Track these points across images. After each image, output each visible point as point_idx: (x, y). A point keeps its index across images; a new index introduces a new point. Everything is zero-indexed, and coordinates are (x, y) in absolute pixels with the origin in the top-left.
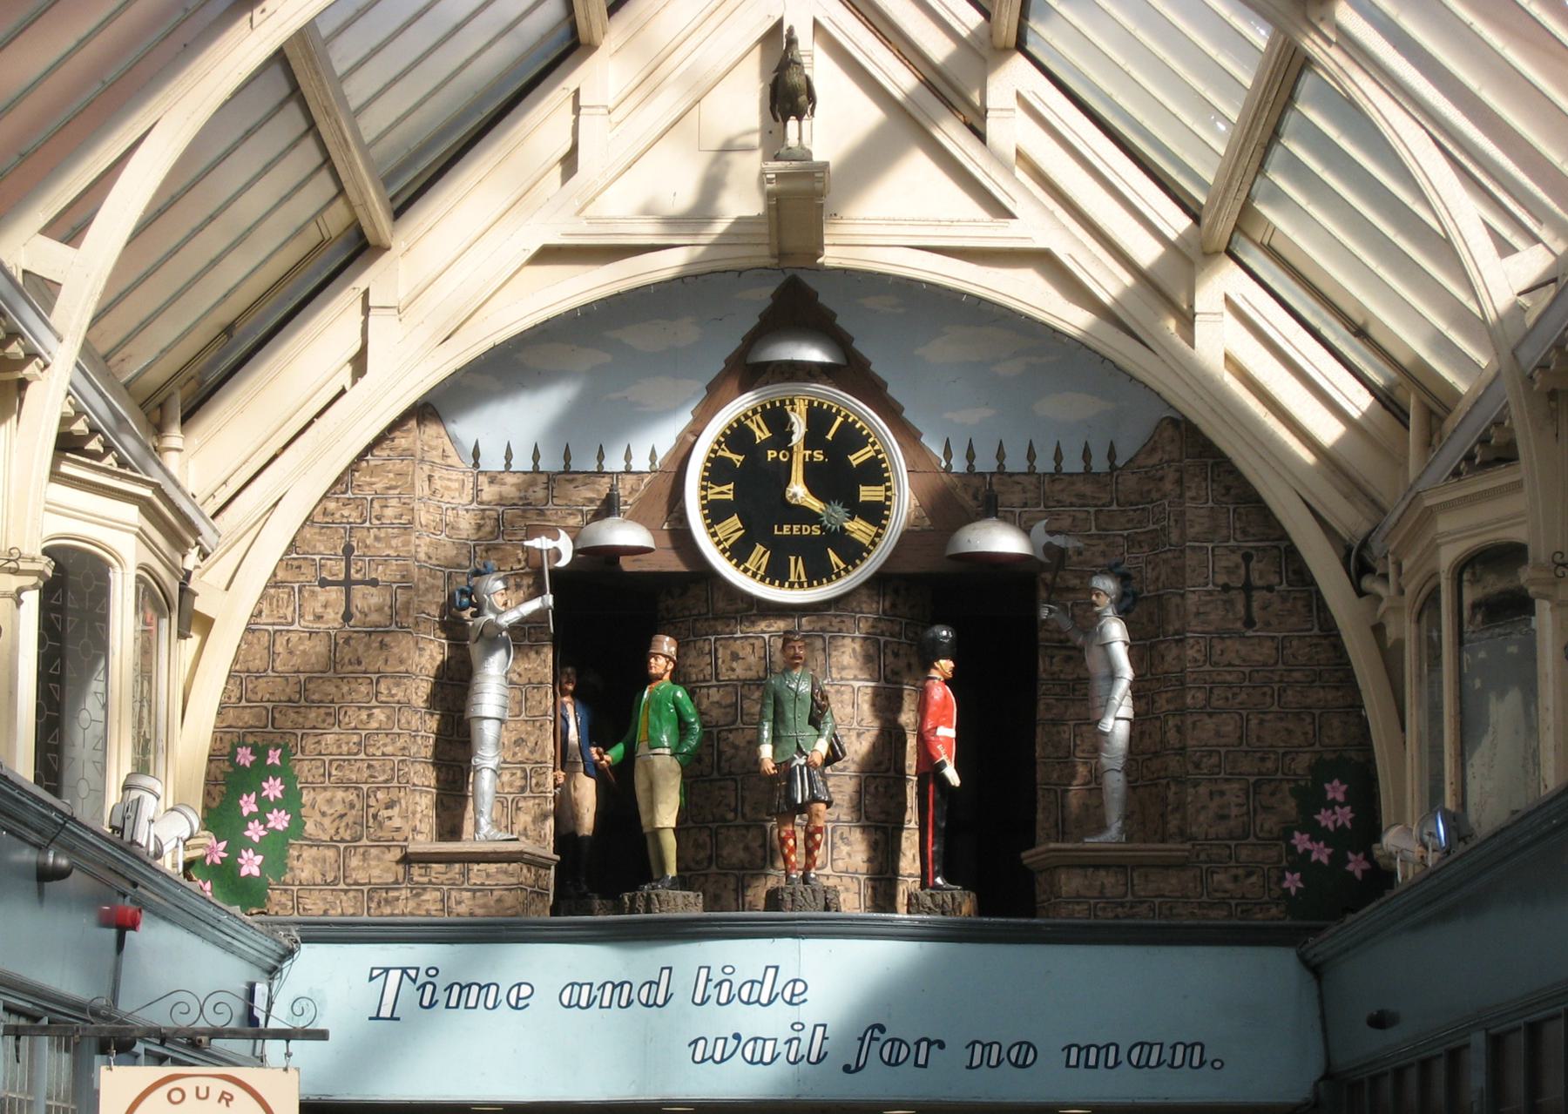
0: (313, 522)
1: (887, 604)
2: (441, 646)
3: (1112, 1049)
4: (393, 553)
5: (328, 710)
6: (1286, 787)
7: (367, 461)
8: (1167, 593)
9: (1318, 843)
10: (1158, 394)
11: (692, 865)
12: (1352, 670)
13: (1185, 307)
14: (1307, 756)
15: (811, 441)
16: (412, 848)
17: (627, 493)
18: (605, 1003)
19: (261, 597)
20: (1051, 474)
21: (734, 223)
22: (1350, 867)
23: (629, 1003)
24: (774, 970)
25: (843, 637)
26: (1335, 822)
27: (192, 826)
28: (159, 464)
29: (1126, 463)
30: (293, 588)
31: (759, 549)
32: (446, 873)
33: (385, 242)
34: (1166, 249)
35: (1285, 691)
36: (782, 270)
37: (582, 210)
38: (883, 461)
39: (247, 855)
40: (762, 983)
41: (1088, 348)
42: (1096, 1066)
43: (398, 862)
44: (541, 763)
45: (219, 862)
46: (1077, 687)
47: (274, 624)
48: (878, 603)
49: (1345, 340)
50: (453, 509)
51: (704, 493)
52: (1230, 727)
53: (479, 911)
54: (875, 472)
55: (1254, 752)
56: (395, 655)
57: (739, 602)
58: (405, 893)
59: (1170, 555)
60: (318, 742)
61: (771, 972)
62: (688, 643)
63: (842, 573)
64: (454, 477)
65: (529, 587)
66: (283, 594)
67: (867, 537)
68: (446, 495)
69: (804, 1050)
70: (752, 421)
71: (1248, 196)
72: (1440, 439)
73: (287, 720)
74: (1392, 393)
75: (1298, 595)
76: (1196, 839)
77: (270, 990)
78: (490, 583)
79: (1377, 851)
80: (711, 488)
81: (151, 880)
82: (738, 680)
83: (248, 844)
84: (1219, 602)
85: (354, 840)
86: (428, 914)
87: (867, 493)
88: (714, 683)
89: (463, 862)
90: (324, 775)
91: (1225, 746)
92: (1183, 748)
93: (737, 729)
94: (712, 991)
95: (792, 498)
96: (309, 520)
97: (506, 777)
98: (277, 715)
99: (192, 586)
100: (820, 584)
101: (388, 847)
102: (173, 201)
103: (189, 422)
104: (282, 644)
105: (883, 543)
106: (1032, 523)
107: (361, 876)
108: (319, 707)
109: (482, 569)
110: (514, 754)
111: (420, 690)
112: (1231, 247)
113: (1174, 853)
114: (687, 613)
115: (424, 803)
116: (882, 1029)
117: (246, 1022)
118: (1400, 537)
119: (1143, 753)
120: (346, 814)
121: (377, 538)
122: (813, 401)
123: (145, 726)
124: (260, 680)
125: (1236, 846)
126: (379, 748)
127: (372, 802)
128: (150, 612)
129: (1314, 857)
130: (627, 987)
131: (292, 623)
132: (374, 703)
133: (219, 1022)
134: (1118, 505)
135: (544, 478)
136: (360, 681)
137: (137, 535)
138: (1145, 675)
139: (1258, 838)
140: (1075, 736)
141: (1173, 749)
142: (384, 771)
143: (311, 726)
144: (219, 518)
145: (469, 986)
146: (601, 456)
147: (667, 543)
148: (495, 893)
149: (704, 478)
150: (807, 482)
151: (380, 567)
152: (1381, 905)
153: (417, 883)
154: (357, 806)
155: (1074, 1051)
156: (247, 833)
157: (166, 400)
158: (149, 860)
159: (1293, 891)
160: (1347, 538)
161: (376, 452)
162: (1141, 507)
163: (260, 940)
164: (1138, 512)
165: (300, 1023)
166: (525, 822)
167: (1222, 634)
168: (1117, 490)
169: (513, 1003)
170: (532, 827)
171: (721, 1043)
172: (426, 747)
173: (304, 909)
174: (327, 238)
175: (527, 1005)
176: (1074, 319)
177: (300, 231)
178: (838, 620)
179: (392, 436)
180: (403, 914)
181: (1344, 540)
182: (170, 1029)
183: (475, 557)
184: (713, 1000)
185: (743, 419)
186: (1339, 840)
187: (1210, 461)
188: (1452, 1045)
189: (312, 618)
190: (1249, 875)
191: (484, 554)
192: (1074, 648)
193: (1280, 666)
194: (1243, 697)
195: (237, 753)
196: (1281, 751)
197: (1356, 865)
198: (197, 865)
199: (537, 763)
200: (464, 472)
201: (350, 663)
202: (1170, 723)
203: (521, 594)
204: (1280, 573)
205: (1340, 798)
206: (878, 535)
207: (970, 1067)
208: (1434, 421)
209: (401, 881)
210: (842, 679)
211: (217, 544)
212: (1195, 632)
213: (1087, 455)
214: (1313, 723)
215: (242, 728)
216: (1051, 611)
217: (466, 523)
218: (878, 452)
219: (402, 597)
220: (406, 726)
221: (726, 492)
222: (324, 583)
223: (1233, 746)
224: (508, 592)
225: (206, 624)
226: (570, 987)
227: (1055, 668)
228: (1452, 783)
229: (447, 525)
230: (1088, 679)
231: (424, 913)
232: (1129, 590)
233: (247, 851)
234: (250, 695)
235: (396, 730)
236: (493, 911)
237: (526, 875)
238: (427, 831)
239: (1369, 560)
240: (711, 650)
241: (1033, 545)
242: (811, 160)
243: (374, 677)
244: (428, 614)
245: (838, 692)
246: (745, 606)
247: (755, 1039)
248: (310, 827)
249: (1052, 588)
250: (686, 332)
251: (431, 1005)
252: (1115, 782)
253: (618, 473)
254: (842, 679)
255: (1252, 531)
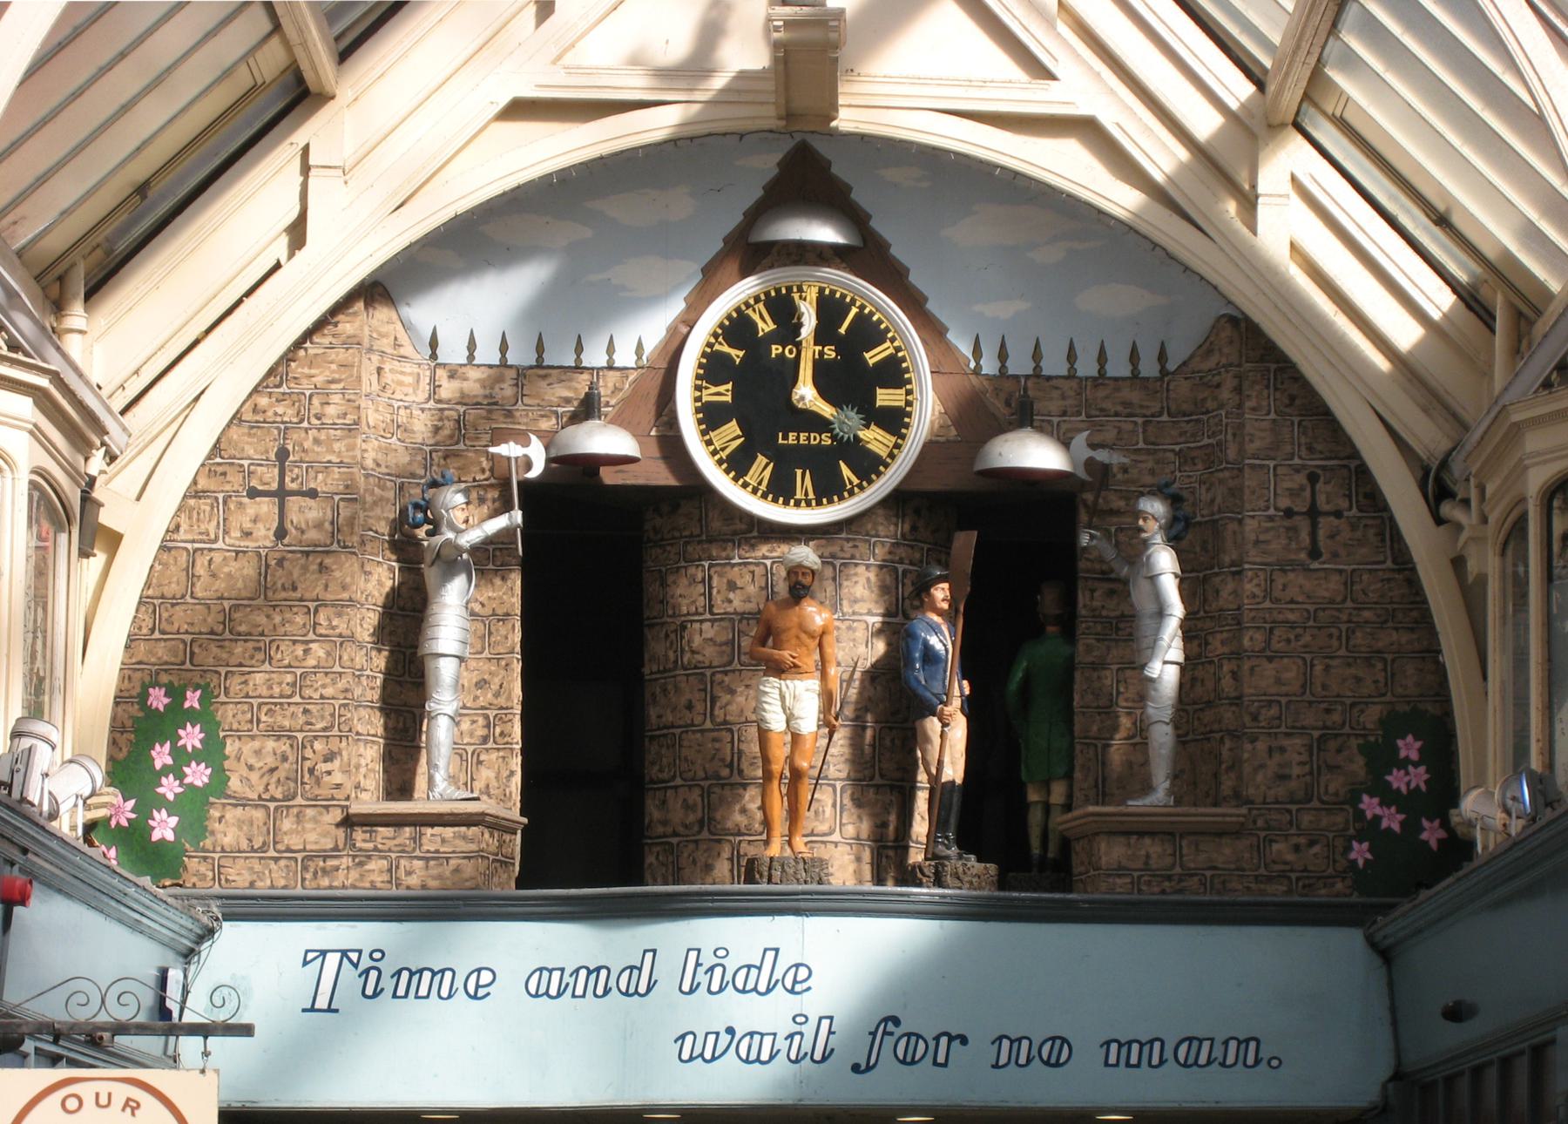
0: (241, 420)
1: (907, 527)
2: (391, 569)
3: (1157, 1045)
4: (335, 459)
5: (257, 645)
6: (1354, 742)
7: (306, 349)
8: (1222, 519)
9: (1389, 807)
10: (1215, 288)
11: (681, 830)
12: (1428, 610)
13: (1247, 187)
14: (1379, 707)
15: (821, 336)
16: (355, 809)
17: (609, 392)
18: (579, 991)
19: (179, 510)
20: (1094, 379)
21: (735, 78)
22: (1424, 836)
23: (607, 991)
24: (773, 953)
25: (856, 565)
26: (1408, 784)
27: (93, 781)
28: (58, 349)
29: (1179, 367)
30: (217, 499)
31: (761, 460)
32: (394, 838)
33: (328, 89)
34: (1227, 120)
35: (1354, 632)
36: (791, 134)
37: (559, 58)
38: (903, 359)
39: (160, 815)
40: (759, 968)
41: (1137, 232)
42: (1138, 1065)
43: (338, 825)
44: (507, 708)
45: (125, 824)
46: (1122, 625)
47: (193, 541)
48: (896, 525)
49: (1425, 228)
50: (406, 408)
51: (698, 394)
52: (1292, 673)
53: (433, 883)
54: (894, 373)
55: (1320, 702)
56: (337, 579)
57: (737, 521)
58: (346, 862)
59: (1227, 474)
60: (245, 682)
61: (771, 955)
62: (678, 568)
63: (856, 489)
64: (408, 370)
65: (494, 501)
66: (205, 505)
67: (884, 448)
68: (397, 392)
69: (807, 1047)
70: (754, 310)
71: (1319, 60)
72: (1530, 345)
73: (207, 658)
74: (1477, 290)
75: (1370, 522)
76: (1252, 802)
77: (185, 977)
78: (449, 496)
79: (1455, 820)
80: (706, 388)
81: (43, 845)
82: (736, 613)
83: (161, 802)
84: (1281, 530)
85: (286, 799)
86: (374, 887)
87: (886, 397)
88: (708, 616)
89: (414, 825)
90: (251, 721)
91: (1286, 695)
92: (1239, 698)
93: (733, 671)
94: (702, 978)
95: (798, 401)
96: (236, 418)
97: (466, 725)
98: (196, 650)
99: (97, 494)
100: (830, 502)
101: (327, 807)
102: (77, 33)
103: (92, 299)
104: (203, 565)
105: (903, 455)
106: (1069, 435)
107: (295, 842)
108: (246, 641)
109: (439, 479)
110: (476, 698)
111: (365, 622)
112: (1299, 120)
113: (1228, 819)
114: (677, 534)
115: (369, 757)
116: (896, 1021)
117: (157, 1015)
118: (1483, 458)
119: (1195, 703)
120: (277, 768)
121: (317, 441)
122: (824, 289)
123: (39, 663)
124: (177, 608)
125: (1298, 810)
126: (316, 690)
127: (308, 753)
128: (46, 525)
129: (1384, 824)
130: (604, 973)
131: (216, 540)
132: (311, 636)
133: (123, 1015)
134: (1169, 415)
135: (512, 373)
136: (295, 609)
137: (31, 433)
138: (1198, 612)
139: (1323, 802)
140: (1118, 682)
141: (1227, 698)
142: (323, 717)
143: (237, 663)
144: (129, 415)
145: (421, 971)
146: (579, 349)
147: (654, 451)
148: (452, 862)
149: (698, 377)
150: (818, 383)
151: (320, 476)
152: (1459, 879)
153: (360, 850)
154: (291, 758)
155: (1114, 1047)
156: (160, 790)
157: (67, 272)
158: (42, 822)
159: (1361, 862)
160: (1425, 457)
161: (316, 339)
162: (1194, 417)
163: (173, 917)
164: (1192, 424)
165: (221, 1016)
166: (488, 778)
167: (1284, 567)
168: (1167, 398)
169: (472, 992)
170: (496, 784)
171: (712, 1038)
172: (373, 688)
173: (227, 880)
174: (259, 83)
175: (488, 994)
176: (1122, 199)
177: (227, 73)
178: (851, 544)
179: (336, 319)
180: (344, 887)
181: (1419, 459)
182: (65, 1023)
183: (431, 465)
184: (704, 987)
185: (743, 308)
186: (1408, 803)
187: (1273, 366)
188: (1536, 1041)
189: (238, 534)
190: (1312, 843)
191: (442, 462)
192: (1118, 580)
193: (1349, 604)
194: (1307, 638)
195: (149, 695)
196: (1348, 701)
197: (1431, 834)
198: (100, 828)
199: (501, 708)
200: (419, 365)
201: (284, 588)
202: (1225, 668)
203: (485, 510)
204: (1350, 497)
205: (1414, 756)
206: (897, 446)
207: (996, 1066)
208: (1523, 323)
209: (341, 846)
210: (854, 613)
211: (127, 445)
212: (1254, 564)
213: (1134, 357)
214: (1385, 670)
215: (154, 665)
216: (1092, 537)
217: (421, 426)
218: (898, 349)
219: (345, 512)
220: (348, 664)
221: (723, 393)
222: (253, 493)
223: (1295, 695)
224: (471, 507)
225: (113, 541)
226: (538, 973)
227: (1096, 604)
228: (1538, 741)
229: (398, 427)
230: (1133, 616)
231: (368, 885)
232: (1180, 514)
233: (159, 811)
234: (164, 625)
235: (337, 669)
236: (449, 883)
237: (489, 840)
238: (372, 788)
239: (1449, 482)
240: (703, 581)
241: (1073, 460)
242: (824, 5)
243: (312, 605)
244: (376, 532)
245: (849, 628)
246: (743, 527)
247: (751, 1034)
248: (235, 784)
249: (1094, 511)
250: (679, 204)
251: (376, 994)
252: (1162, 737)
253: (599, 369)
254: (854, 613)
255: (1319, 447)
